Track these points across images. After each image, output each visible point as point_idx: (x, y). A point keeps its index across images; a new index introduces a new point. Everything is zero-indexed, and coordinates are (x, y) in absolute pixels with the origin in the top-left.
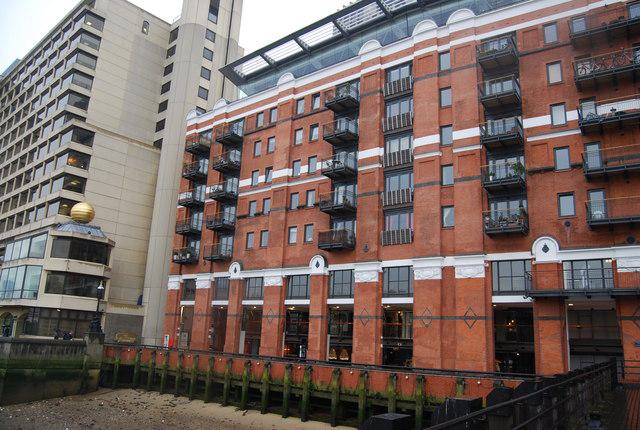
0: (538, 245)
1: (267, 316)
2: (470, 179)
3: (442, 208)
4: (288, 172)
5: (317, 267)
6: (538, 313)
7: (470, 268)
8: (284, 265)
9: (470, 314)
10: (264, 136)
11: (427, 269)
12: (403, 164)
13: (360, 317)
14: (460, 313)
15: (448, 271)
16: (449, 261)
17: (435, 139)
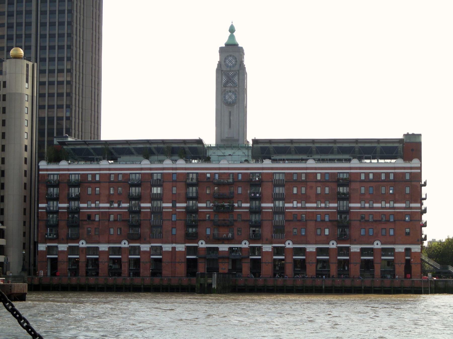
0: (200, 242)
2: (181, 220)
3: (172, 228)
4: (108, 205)
5: (125, 244)
6: (199, 261)
7: (181, 247)
8: (109, 243)
9: (180, 261)
11: (167, 247)
12: (157, 212)
13: (143, 262)
14: (177, 261)
15: (174, 248)
16: (174, 245)
17: (170, 205)
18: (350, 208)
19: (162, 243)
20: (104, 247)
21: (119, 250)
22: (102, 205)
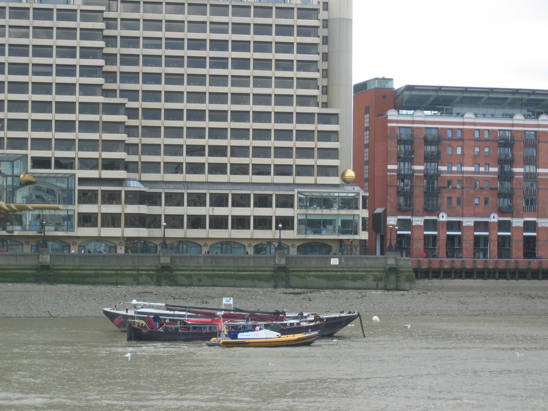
1: (466, 240)
4: (472, 169)
5: (494, 218)
8: (475, 215)
10: (454, 144)
13: (516, 241)
18: (414, 171)
19: (538, 217)
20: (468, 222)
21: (485, 226)
22: (465, 169)
